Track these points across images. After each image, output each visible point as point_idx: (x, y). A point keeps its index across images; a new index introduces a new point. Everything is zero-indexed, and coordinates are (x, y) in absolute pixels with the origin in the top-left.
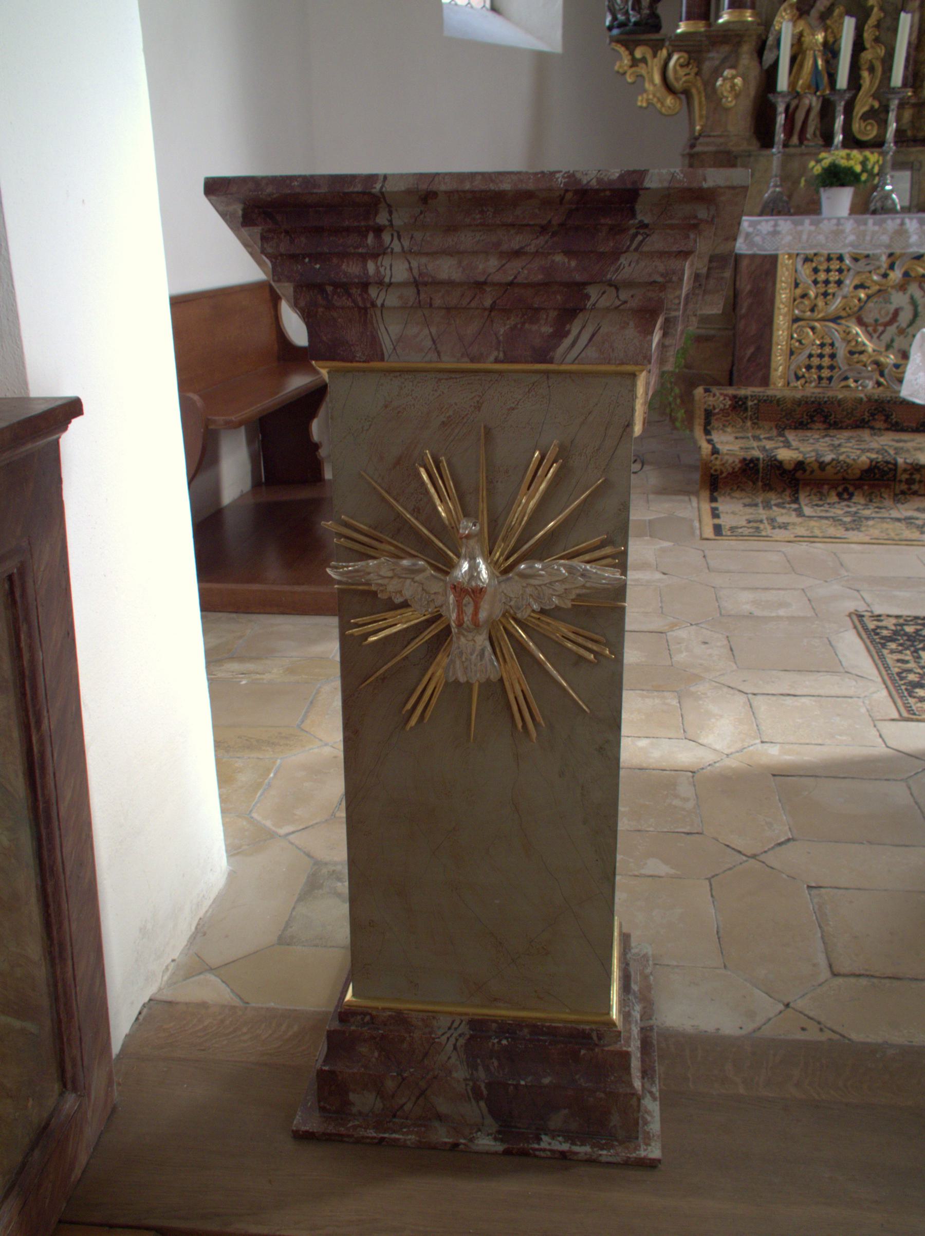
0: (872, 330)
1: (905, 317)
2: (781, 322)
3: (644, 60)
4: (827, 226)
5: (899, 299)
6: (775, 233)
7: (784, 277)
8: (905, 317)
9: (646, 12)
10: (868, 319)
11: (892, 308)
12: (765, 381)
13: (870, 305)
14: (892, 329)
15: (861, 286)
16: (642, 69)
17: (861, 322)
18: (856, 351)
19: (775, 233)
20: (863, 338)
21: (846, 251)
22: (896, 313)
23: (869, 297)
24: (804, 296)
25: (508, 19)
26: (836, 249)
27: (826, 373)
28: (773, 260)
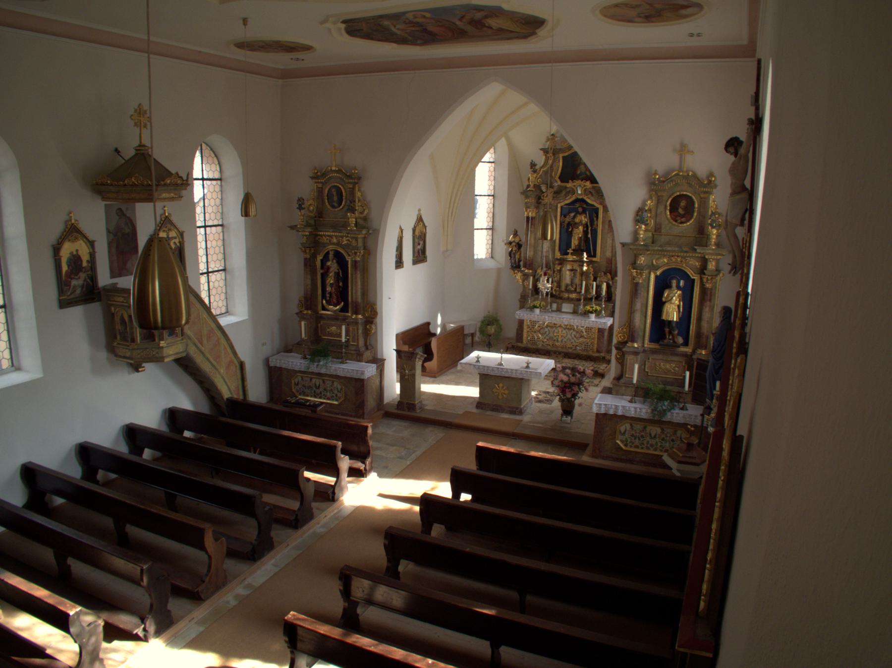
0: (542, 334)
1: (547, 333)
2: (525, 331)
3: (516, 273)
4: (533, 315)
5: (546, 330)
6: (523, 316)
7: (525, 323)
8: (547, 333)
9: (517, 264)
10: (541, 332)
11: (545, 331)
12: (522, 342)
13: (541, 330)
14: (545, 335)
15: (539, 327)
16: (516, 274)
17: (540, 333)
18: (539, 338)
19: (523, 316)
20: (540, 336)
21: (536, 320)
22: (546, 332)
23: (541, 329)
24: (529, 327)
25: (494, 259)
26: (534, 320)
27: (534, 342)
28: (523, 320)
